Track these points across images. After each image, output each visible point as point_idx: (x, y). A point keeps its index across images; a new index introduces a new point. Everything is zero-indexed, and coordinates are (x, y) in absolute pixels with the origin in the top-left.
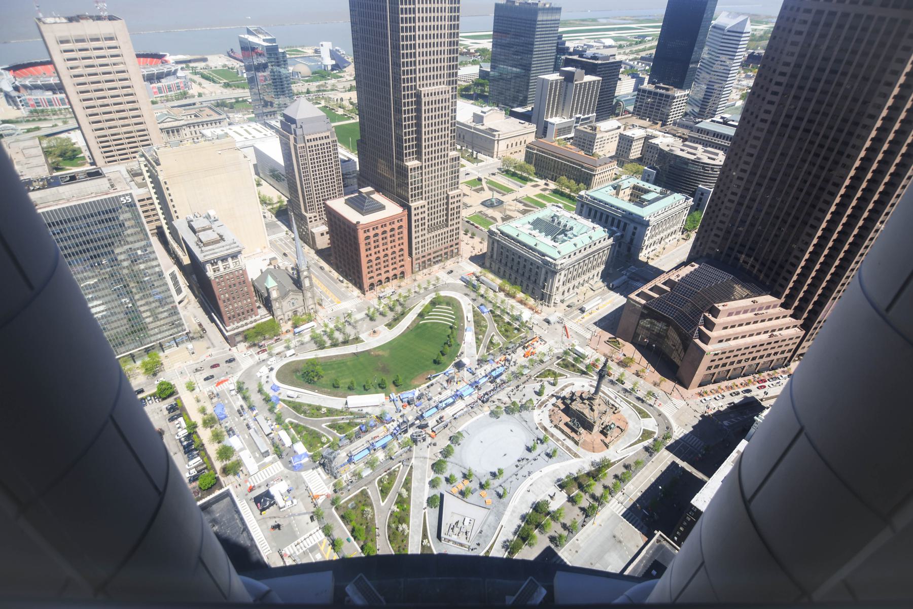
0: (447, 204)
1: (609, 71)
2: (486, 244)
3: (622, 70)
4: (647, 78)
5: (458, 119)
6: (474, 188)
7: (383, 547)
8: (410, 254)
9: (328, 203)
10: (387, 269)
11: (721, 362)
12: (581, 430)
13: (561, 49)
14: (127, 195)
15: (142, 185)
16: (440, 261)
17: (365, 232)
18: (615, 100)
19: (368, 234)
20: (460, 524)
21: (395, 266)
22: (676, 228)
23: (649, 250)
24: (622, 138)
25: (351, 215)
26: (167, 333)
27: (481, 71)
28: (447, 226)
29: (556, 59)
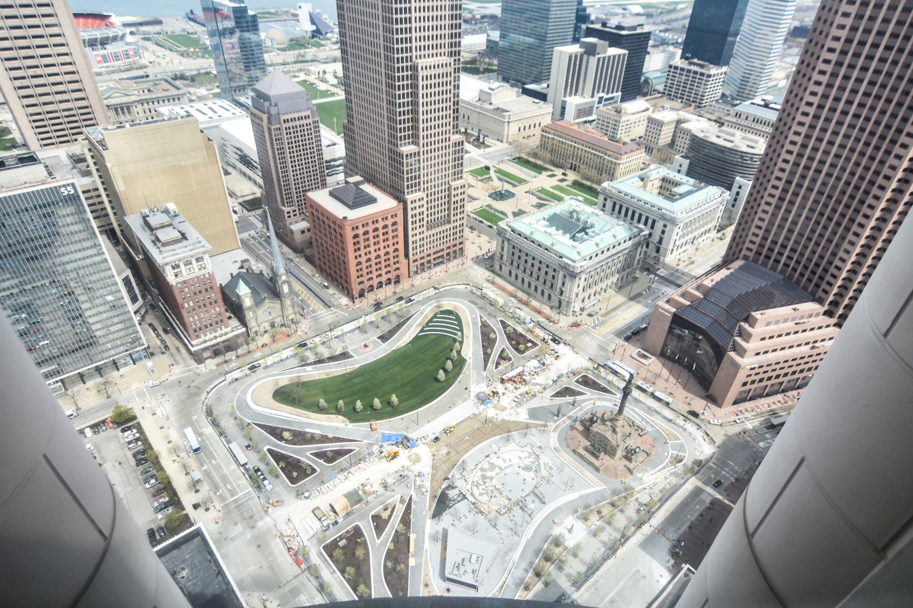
0: (449, 196)
1: (637, 45)
2: (494, 243)
3: (651, 43)
4: (679, 52)
5: (461, 97)
6: (480, 178)
7: (379, 589)
8: (407, 256)
9: (310, 194)
10: (379, 272)
11: (758, 378)
12: (602, 455)
13: (582, 17)
14: (68, 185)
15: (88, 173)
16: (442, 262)
17: (353, 228)
18: (643, 79)
19: (357, 232)
20: (466, 562)
21: (388, 269)
22: (710, 226)
23: (680, 250)
24: (650, 120)
25: (337, 210)
26: (122, 348)
27: (488, 41)
28: (449, 222)
29: (577, 29)
